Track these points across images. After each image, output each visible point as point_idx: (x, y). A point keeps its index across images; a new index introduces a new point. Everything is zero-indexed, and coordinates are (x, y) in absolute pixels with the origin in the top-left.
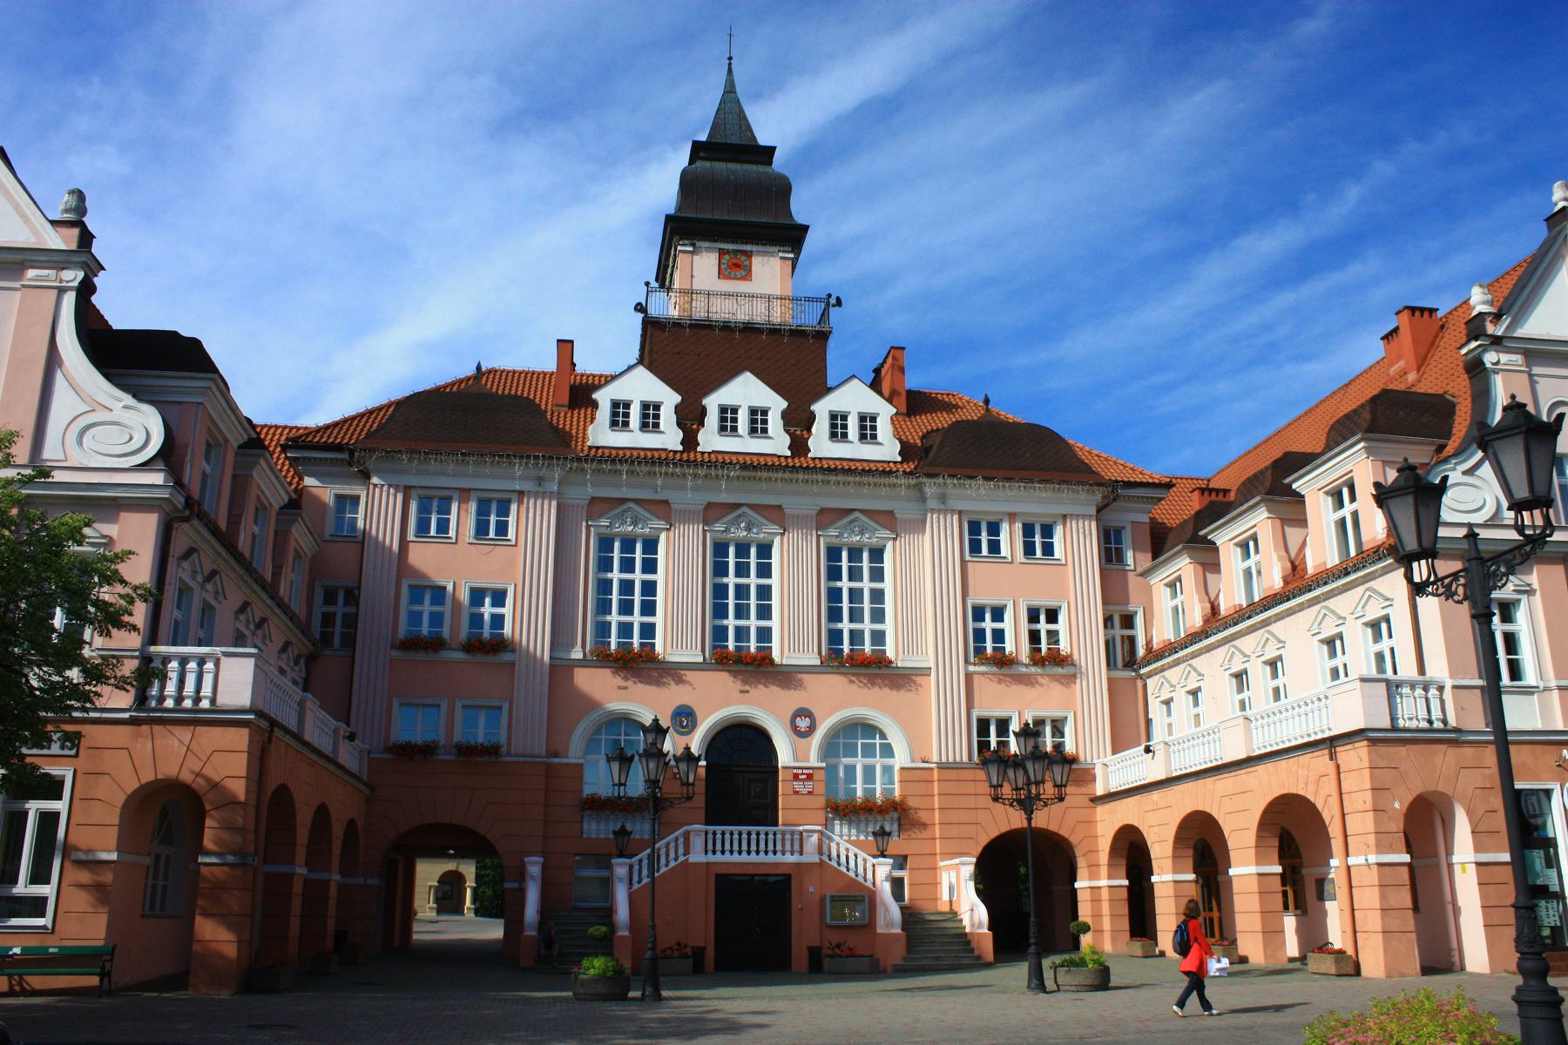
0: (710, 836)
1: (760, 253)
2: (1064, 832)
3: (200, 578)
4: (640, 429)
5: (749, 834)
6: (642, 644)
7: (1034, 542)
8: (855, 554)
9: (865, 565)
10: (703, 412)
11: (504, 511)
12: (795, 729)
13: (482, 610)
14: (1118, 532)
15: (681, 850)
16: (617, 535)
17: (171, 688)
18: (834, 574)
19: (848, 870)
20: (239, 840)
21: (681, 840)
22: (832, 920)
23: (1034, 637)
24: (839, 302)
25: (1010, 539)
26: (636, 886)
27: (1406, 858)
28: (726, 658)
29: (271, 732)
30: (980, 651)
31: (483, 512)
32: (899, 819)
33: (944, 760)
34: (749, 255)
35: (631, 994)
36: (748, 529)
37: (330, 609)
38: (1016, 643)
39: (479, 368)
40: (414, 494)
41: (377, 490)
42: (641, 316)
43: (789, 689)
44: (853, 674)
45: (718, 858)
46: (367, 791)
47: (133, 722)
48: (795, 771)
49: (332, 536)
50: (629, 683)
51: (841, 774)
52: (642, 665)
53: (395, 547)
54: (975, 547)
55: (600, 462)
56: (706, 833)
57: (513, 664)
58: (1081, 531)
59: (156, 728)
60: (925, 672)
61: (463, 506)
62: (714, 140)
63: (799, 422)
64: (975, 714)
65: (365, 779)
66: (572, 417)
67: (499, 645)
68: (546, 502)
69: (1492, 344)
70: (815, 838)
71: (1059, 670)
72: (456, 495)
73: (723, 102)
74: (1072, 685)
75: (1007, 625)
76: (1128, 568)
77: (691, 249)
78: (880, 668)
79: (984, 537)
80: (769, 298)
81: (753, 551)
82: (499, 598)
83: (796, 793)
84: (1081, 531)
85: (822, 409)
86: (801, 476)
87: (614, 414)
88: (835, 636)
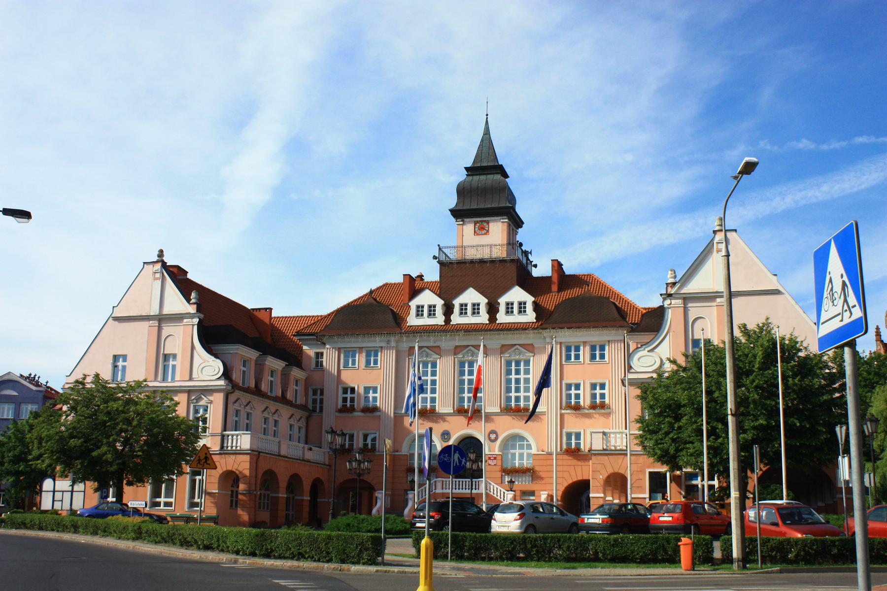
0: (444, 483)
3: (243, 407)
4: (428, 317)
6: (431, 406)
9: (522, 368)
11: (376, 355)
12: (490, 439)
15: (434, 488)
17: (230, 444)
23: (594, 396)
25: (585, 353)
27: (602, 495)
29: (259, 454)
31: (368, 355)
33: (549, 451)
34: (488, 223)
38: (585, 400)
40: (342, 351)
47: (220, 454)
50: (425, 422)
51: (510, 457)
53: (336, 373)
54: (568, 358)
56: (443, 481)
57: (380, 416)
59: (226, 456)
62: (475, 166)
63: (493, 309)
64: (565, 431)
65: (327, 463)
67: (375, 409)
69: (668, 296)
71: (603, 411)
75: (581, 392)
77: (462, 223)
82: (375, 390)
83: (489, 465)
86: (489, 333)
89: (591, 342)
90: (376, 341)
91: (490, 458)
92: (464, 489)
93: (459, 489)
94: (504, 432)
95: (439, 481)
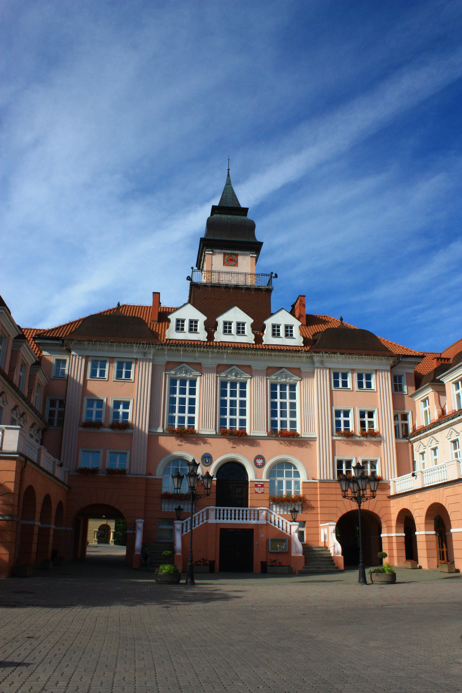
0: (218, 511)
2: (376, 512)
5: (235, 511)
7: (363, 382)
8: (283, 387)
9: (288, 392)
10: (216, 324)
11: (129, 367)
12: (256, 464)
13: (119, 410)
14: (400, 377)
15: (205, 518)
16: (178, 378)
18: (274, 396)
19: (279, 527)
20: (11, 509)
21: (205, 513)
22: (271, 550)
23: (363, 424)
24: (276, 276)
25: (352, 381)
26: (185, 533)
28: (226, 432)
29: (26, 462)
30: (338, 430)
31: (120, 367)
32: (302, 505)
33: (322, 478)
34: (237, 255)
35: (181, 581)
36: (236, 376)
37: (52, 409)
39: (119, 304)
40: (90, 359)
41: (74, 357)
42: (189, 282)
43: (253, 446)
44: (282, 440)
45: (221, 521)
46: (67, 489)
48: (256, 483)
49: (54, 377)
50: (183, 443)
51: (276, 484)
52: (189, 435)
54: (336, 384)
55: (171, 346)
56: (216, 510)
57: (132, 434)
58: (384, 377)
60: (314, 439)
61: (111, 365)
64: (336, 458)
65: (67, 483)
66: (159, 326)
67: (126, 426)
68: (147, 363)
70: (264, 513)
71: (374, 439)
72: (108, 360)
73: (225, 189)
74: (380, 446)
75: (350, 419)
76: (404, 393)
77: (211, 253)
78: (294, 437)
79: (340, 380)
80: (245, 274)
81: (238, 385)
82: (126, 405)
83: (256, 492)
84: (384, 377)
85: (269, 323)
86: (259, 353)
87: (177, 325)
88: (274, 423)
89: (358, 369)
90: (133, 352)
91: (256, 486)
92: (241, 520)
93: (239, 519)
94: (271, 458)
95: (213, 509)
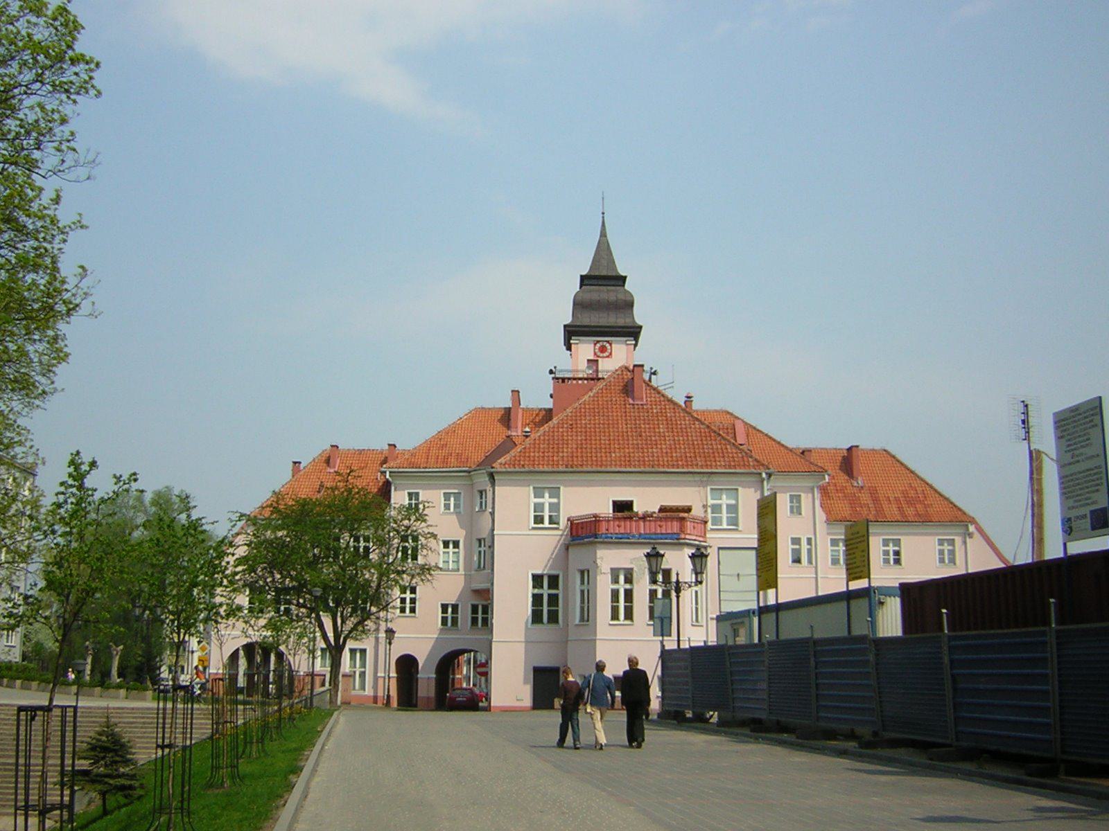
1: (617, 342)
